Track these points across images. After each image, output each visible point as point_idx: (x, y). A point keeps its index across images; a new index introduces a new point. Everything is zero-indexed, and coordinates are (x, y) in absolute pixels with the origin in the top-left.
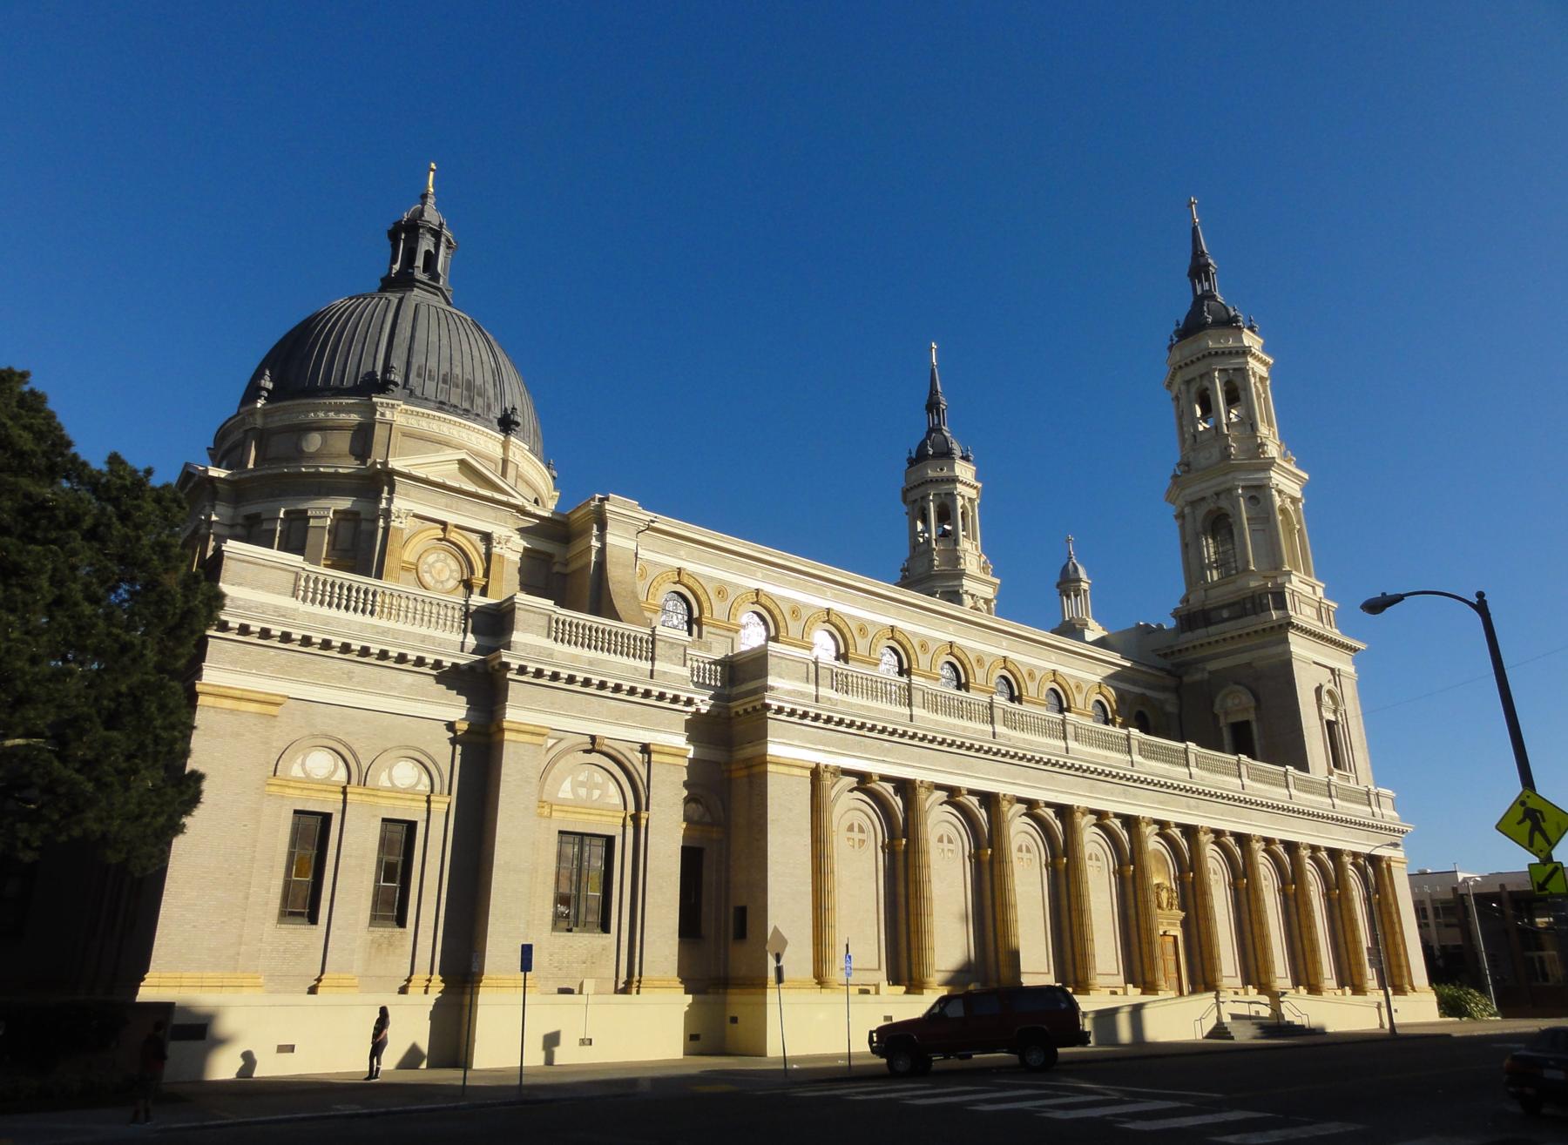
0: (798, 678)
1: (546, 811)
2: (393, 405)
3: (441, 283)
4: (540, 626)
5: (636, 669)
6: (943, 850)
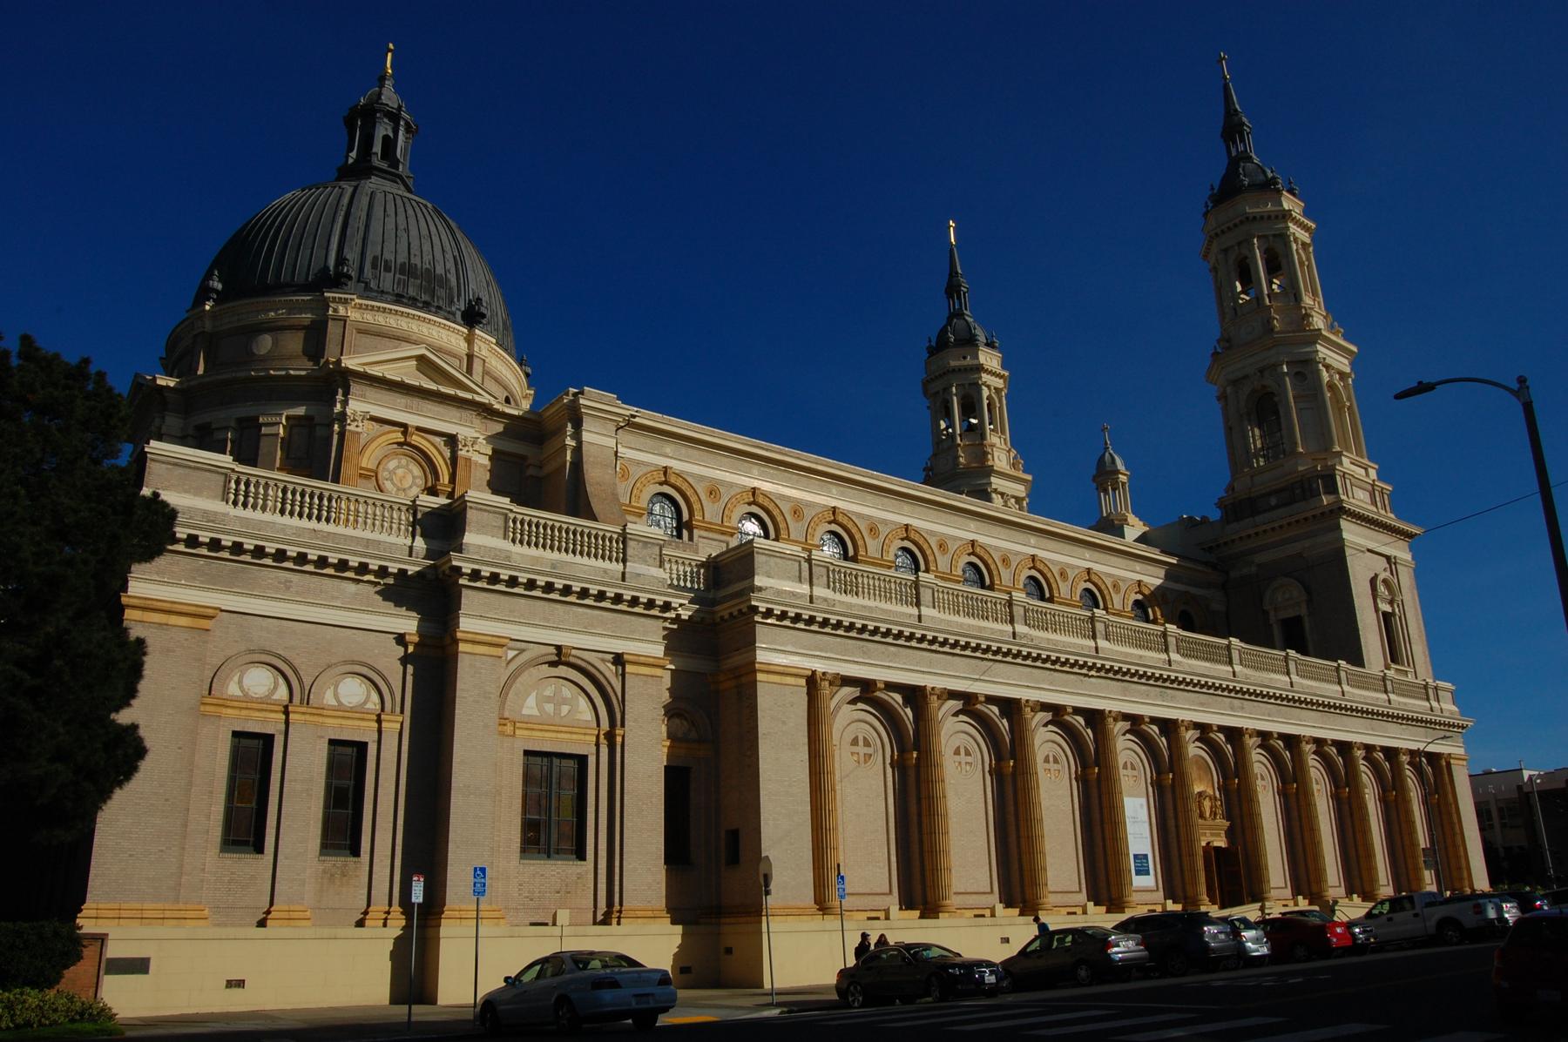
1: (509, 729)
2: (346, 299)
3: (400, 170)
4: (495, 526)
5: (605, 571)
6: (960, 763)
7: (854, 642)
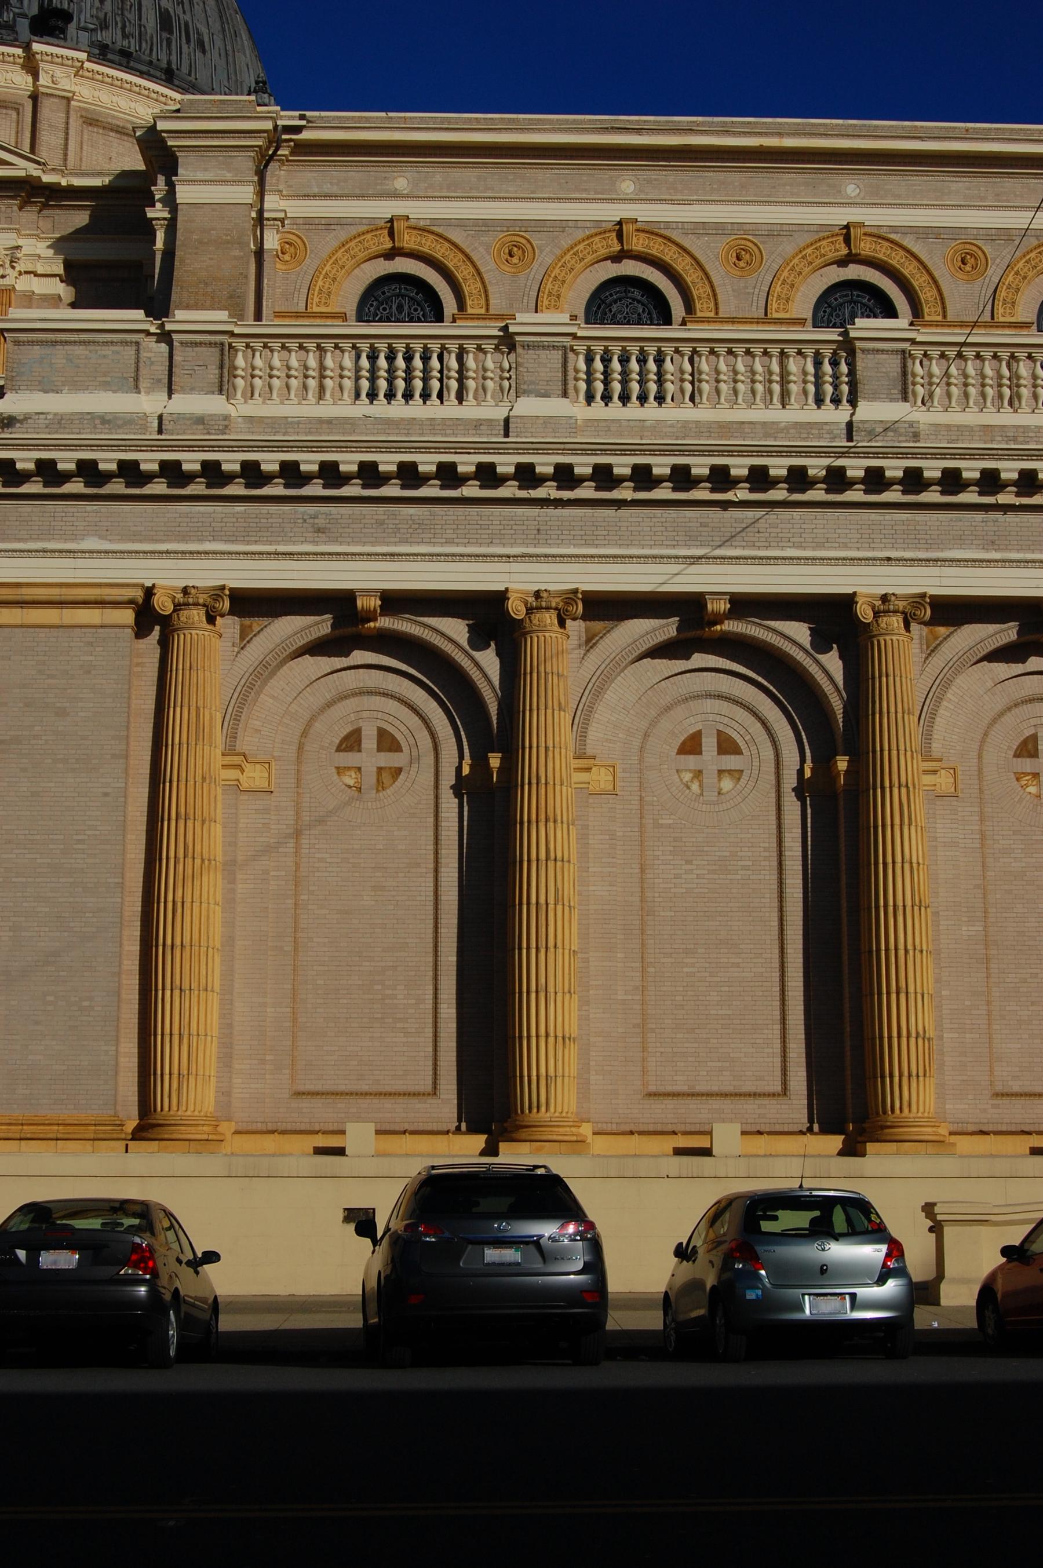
0: (107, 383)
6: (698, 774)
7: (287, 508)
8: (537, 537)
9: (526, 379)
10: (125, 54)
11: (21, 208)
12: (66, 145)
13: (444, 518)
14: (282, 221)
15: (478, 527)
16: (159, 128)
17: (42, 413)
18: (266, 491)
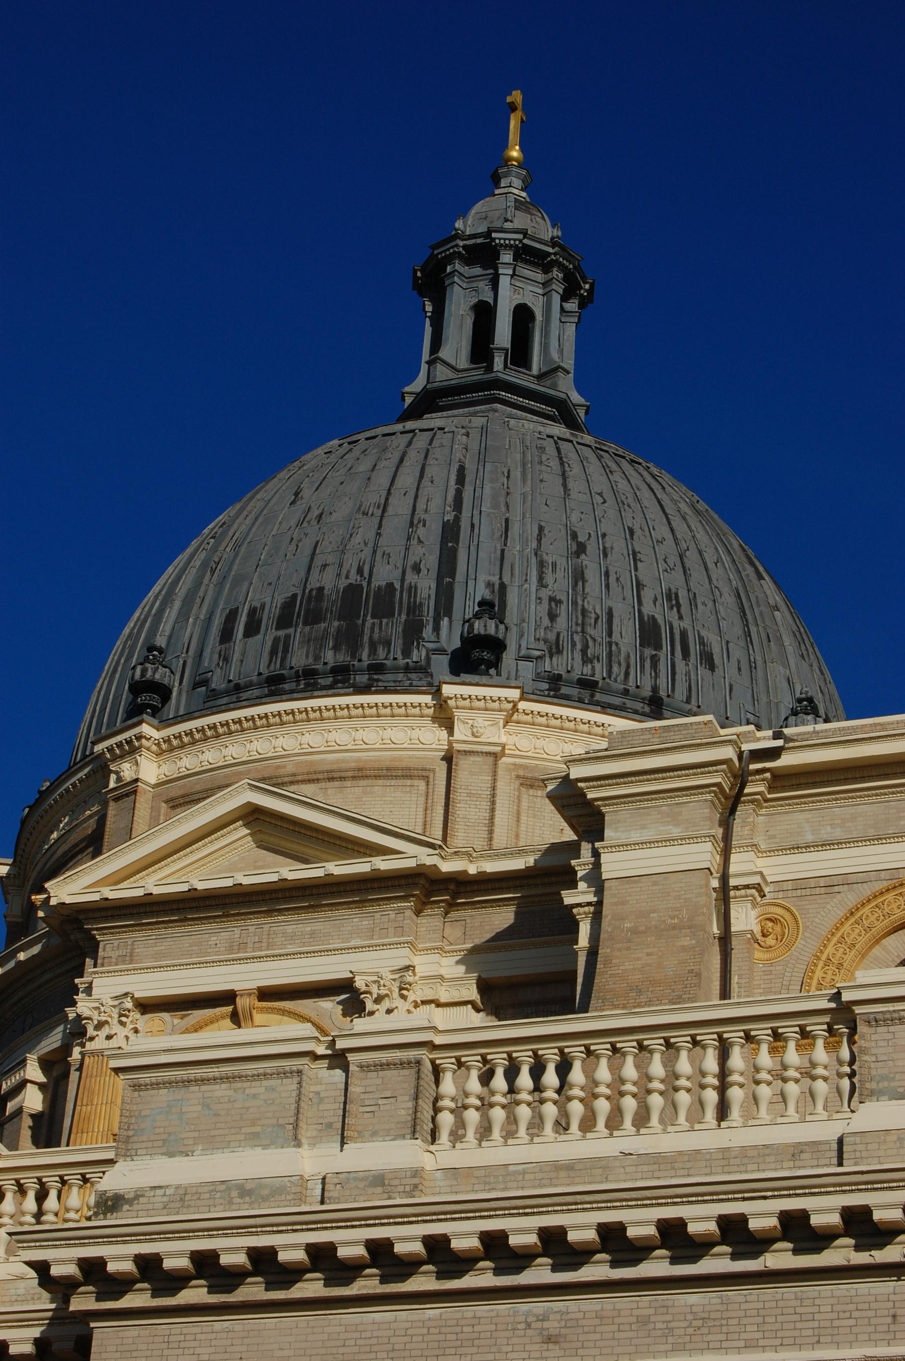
7: (502, 1308)
8: (892, 1328)
9: (874, 1072)
10: (587, 684)
11: (418, 913)
12: (492, 818)
13: (743, 1306)
14: (758, 888)
15: (797, 1317)
16: (572, 777)
17: (160, 1187)
18: (468, 1281)
